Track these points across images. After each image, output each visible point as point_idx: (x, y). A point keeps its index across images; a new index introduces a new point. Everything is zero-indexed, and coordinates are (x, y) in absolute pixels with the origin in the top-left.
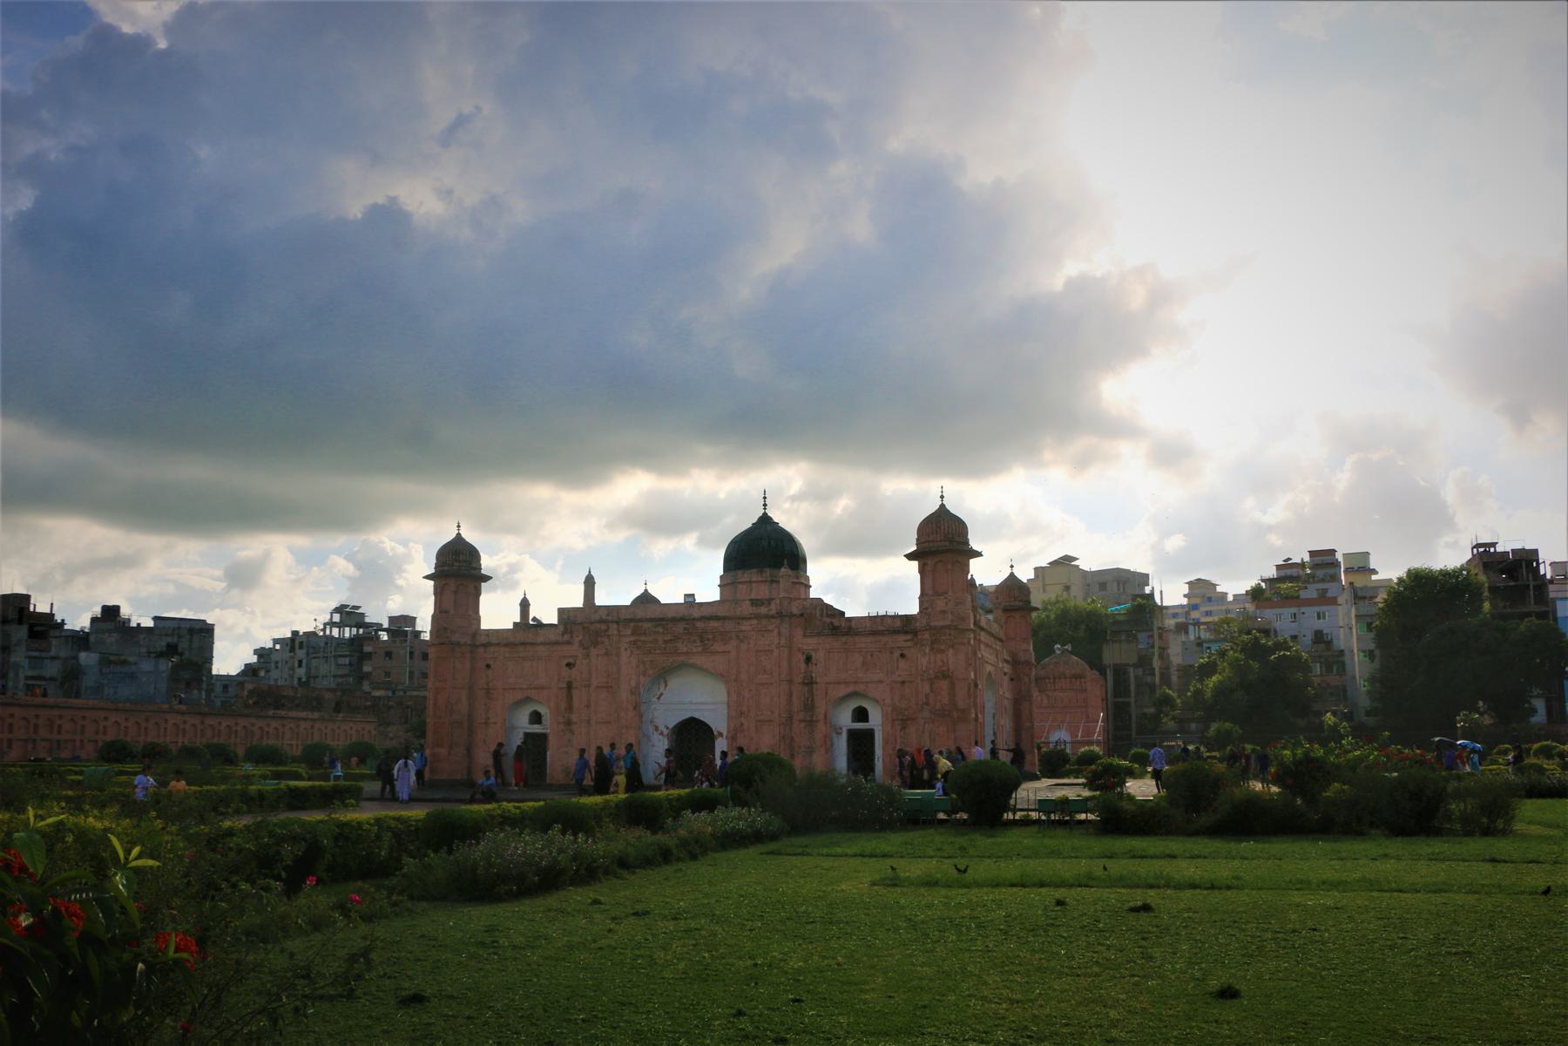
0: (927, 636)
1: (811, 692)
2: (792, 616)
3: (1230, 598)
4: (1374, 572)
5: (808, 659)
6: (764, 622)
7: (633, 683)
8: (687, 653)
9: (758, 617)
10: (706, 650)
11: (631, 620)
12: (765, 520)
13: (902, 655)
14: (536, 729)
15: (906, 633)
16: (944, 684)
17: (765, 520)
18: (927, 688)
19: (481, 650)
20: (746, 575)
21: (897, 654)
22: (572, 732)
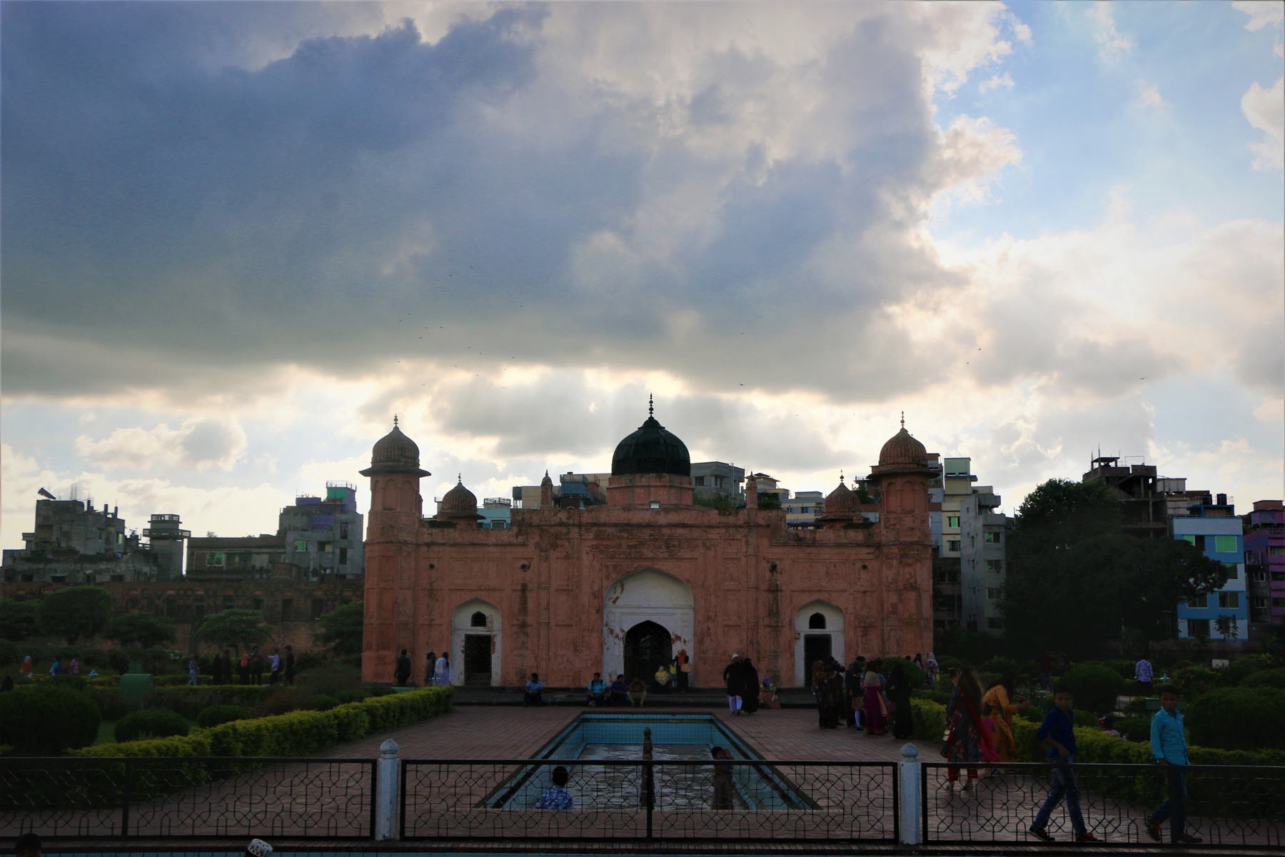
1: (776, 599)
3: (792, 496)
4: (974, 478)
6: (732, 530)
7: (596, 588)
8: (652, 559)
9: (727, 526)
11: (595, 525)
12: (651, 424)
13: (864, 567)
14: (480, 631)
15: (868, 546)
16: (913, 595)
17: (651, 424)
18: (893, 598)
19: (424, 549)
20: (625, 480)
21: (860, 565)
22: (527, 635)
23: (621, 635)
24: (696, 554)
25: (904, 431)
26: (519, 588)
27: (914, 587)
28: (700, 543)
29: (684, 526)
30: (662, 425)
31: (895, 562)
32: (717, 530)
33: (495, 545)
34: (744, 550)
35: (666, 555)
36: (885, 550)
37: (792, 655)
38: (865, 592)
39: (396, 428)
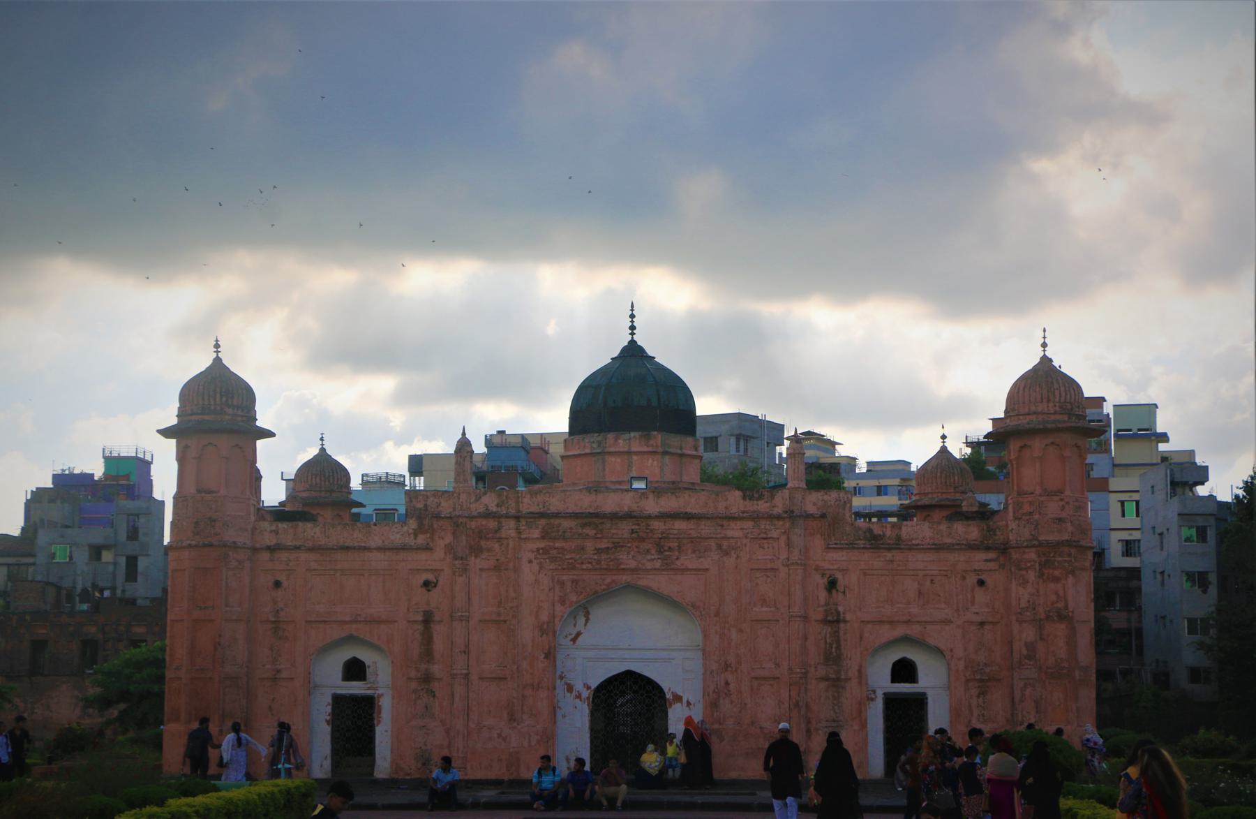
0: (1032, 555)
1: (836, 635)
2: (808, 516)
3: (862, 468)
4: (1164, 437)
5: (832, 584)
6: (764, 524)
7: (544, 617)
9: (756, 517)
10: (668, 567)
11: (542, 515)
12: (633, 352)
13: (981, 583)
14: (356, 688)
15: (988, 549)
16: (1061, 629)
17: (633, 352)
18: (1029, 634)
19: (265, 556)
20: (589, 443)
21: (972, 579)
23: (585, 694)
24: (706, 563)
25: (1046, 361)
26: (420, 618)
27: (1063, 616)
28: (713, 544)
29: (688, 517)
30: (650, 353)
31: (1031, 575)
32: (739, 524)
33: (379, 549)
34: (784, 556)
35: (658, 564)
36: (1015, 555)
37: (864, 725)
38: (982, 624)
39: (218, 361)
